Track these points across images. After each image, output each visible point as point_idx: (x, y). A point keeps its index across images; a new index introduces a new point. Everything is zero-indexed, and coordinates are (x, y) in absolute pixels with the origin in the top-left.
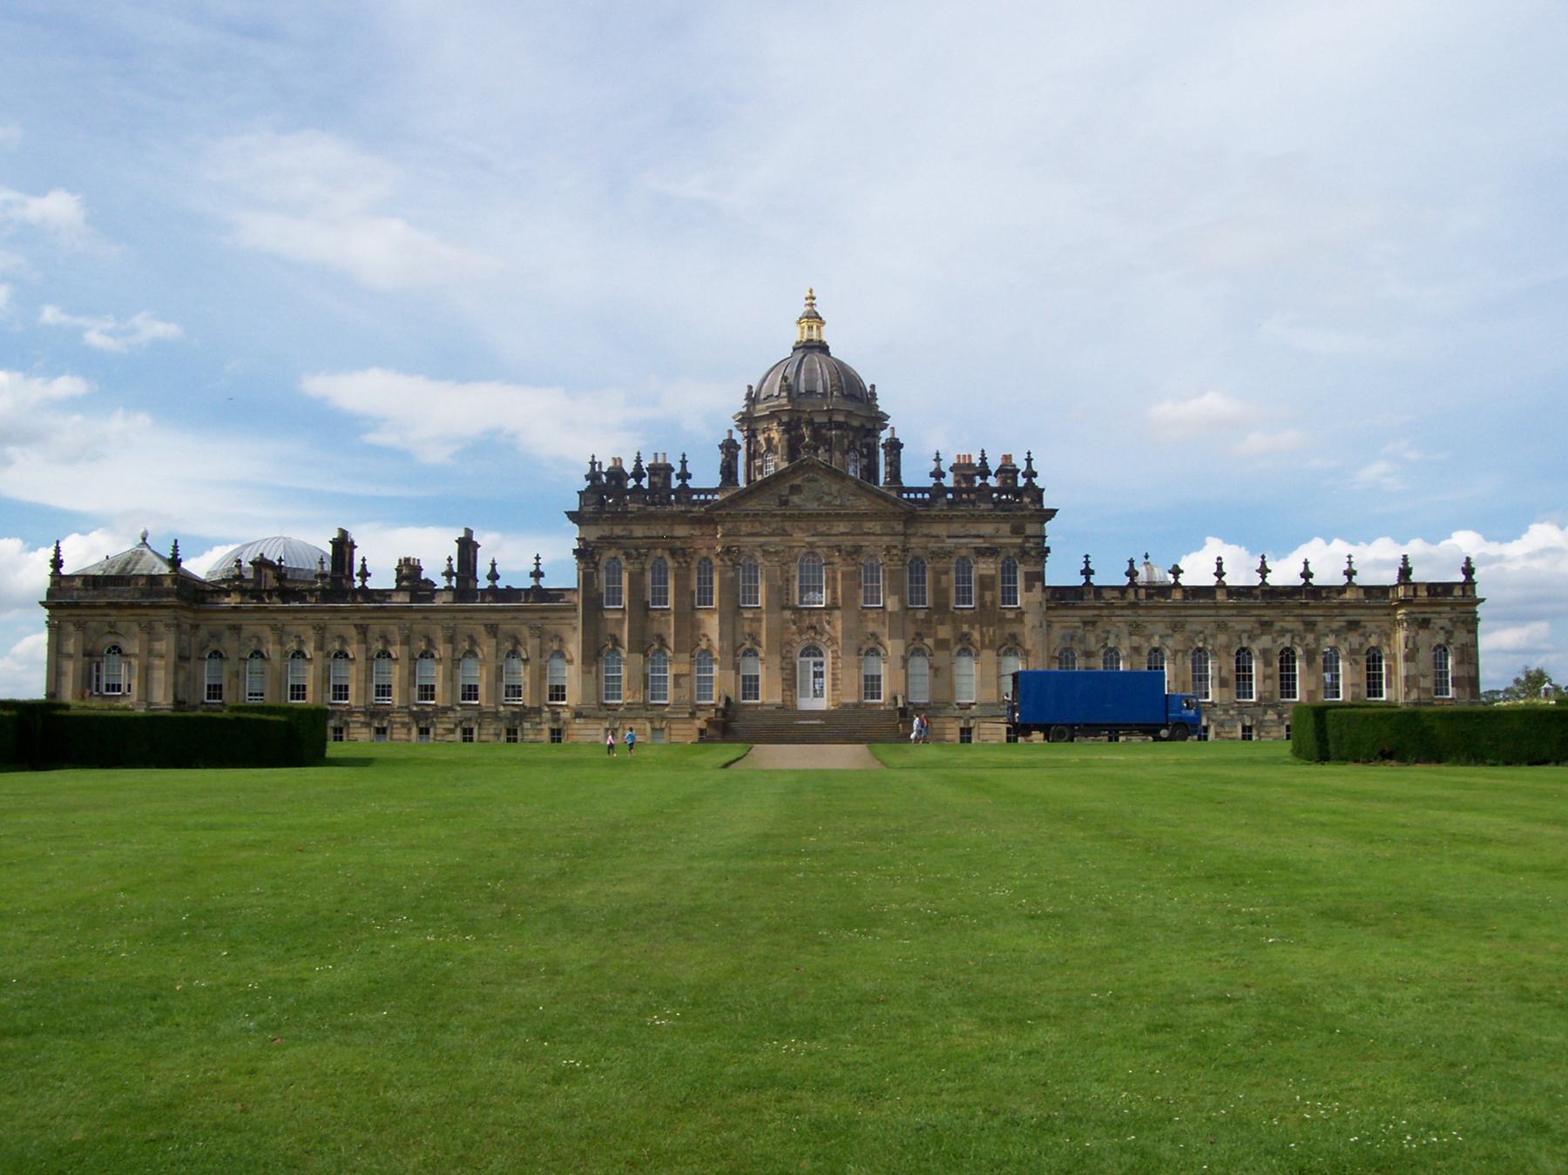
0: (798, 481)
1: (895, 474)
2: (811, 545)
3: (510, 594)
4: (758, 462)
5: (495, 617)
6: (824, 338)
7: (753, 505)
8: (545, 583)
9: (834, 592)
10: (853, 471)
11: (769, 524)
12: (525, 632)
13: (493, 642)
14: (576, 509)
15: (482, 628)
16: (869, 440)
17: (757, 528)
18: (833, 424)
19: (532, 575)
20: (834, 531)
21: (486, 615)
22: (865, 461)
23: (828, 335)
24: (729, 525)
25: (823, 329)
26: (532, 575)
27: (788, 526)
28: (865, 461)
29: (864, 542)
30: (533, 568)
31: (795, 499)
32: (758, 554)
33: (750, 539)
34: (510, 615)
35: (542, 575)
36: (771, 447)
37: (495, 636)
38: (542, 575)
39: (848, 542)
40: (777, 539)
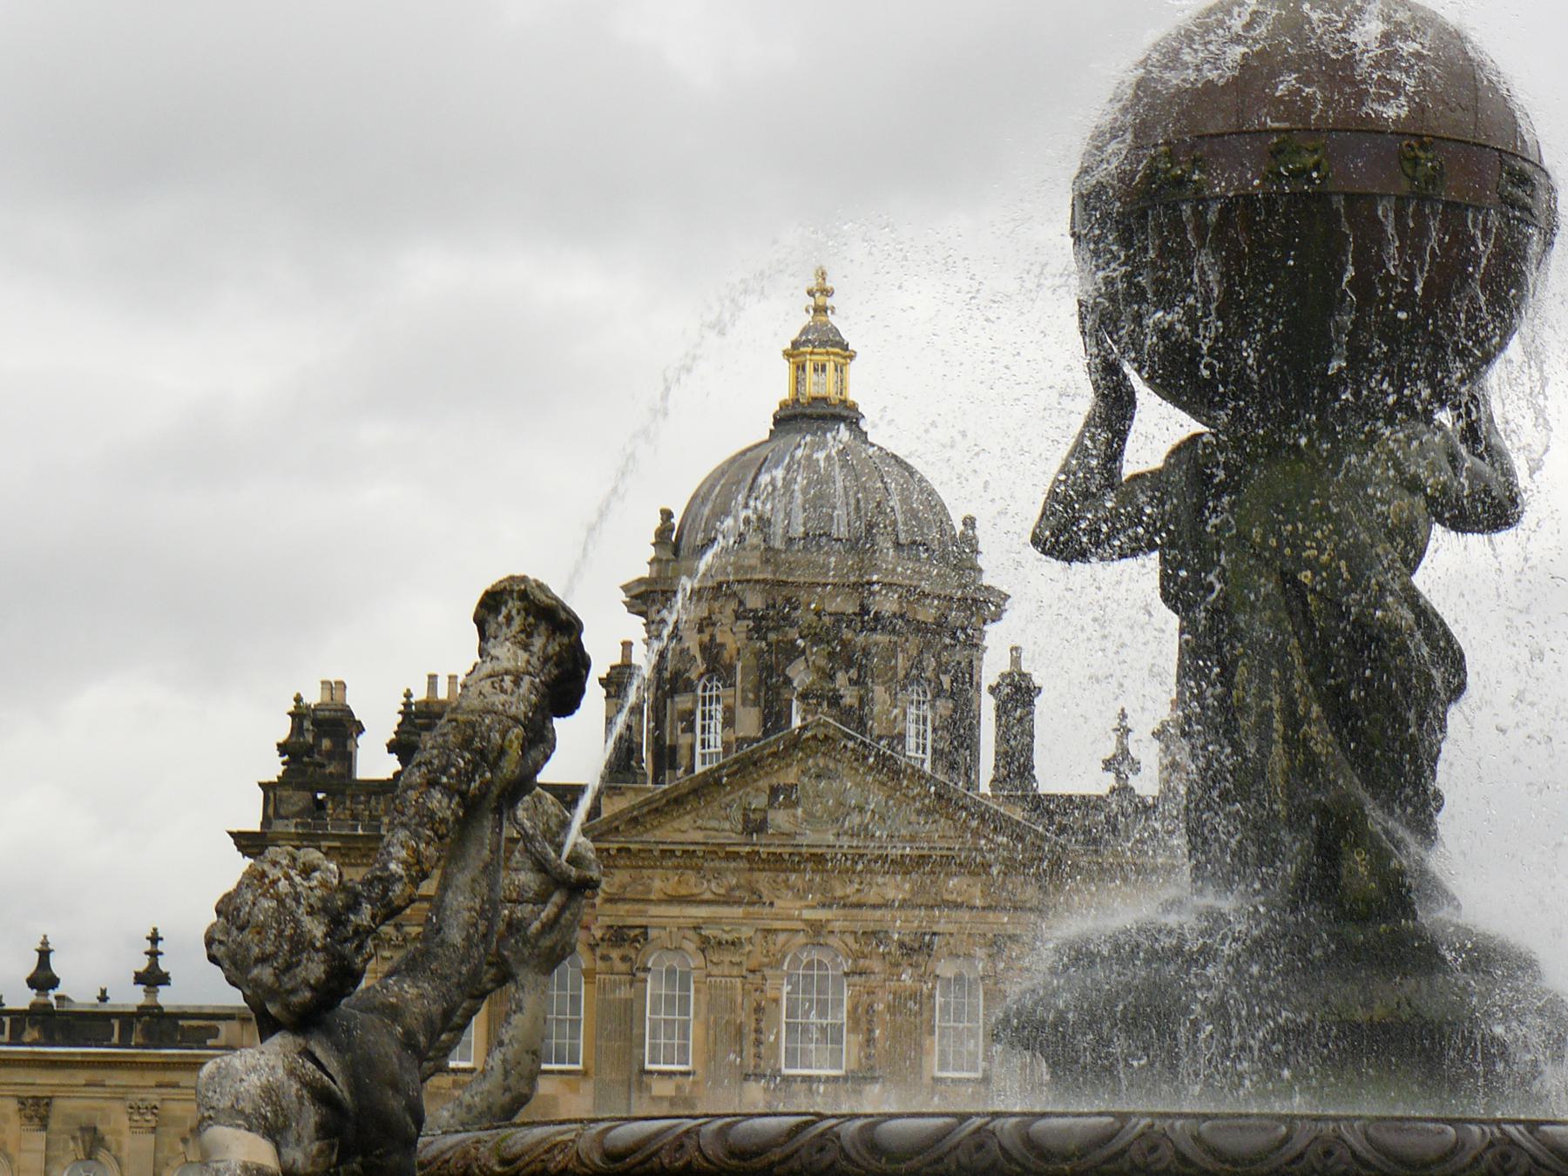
0: (790, 776)
1: (1017, 764)
2: (817, 928)
3: (88, 1025)
4: (683, 702)
5: (44, 1081)
6: (853, 395)
7: (683, 830)
8: (167, 998)
9: (870, 1041)
10: (918, 750)
11: (718, 874)
12: (116, 1122)
13: (38, 1140)
14: (254, 825)
15: (13, 1105)
16: (960, 655)
17: (692, 883)
18: (866, 619)
19: (140, 978)
20: (872, 896)
21: (21, 1076)
22: (945, 706)
23: (861, 387)
24: (621, 877)
25: (854, 370)
26: (140, 978)
27: (763, 880)
28: (945, 706)
29: (944, 922)
30: (143, 964)
31: (780, 819)
32: (690, 946)
33: (674, 910)
34: (82, 1076)
35: (164, 979)
36: (717, 667)
37: (44, 1126)
38: (164, 979)
39: (900, 925)
40: (738, 911)
